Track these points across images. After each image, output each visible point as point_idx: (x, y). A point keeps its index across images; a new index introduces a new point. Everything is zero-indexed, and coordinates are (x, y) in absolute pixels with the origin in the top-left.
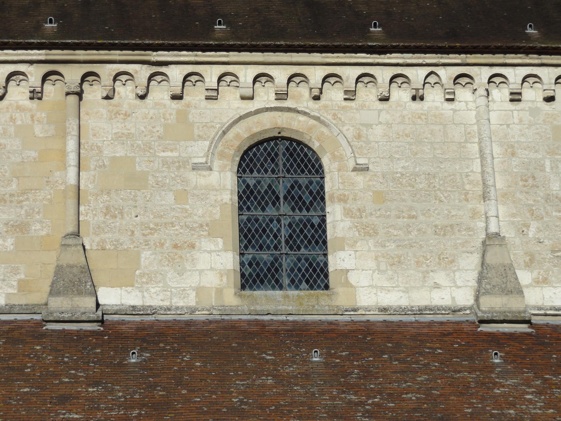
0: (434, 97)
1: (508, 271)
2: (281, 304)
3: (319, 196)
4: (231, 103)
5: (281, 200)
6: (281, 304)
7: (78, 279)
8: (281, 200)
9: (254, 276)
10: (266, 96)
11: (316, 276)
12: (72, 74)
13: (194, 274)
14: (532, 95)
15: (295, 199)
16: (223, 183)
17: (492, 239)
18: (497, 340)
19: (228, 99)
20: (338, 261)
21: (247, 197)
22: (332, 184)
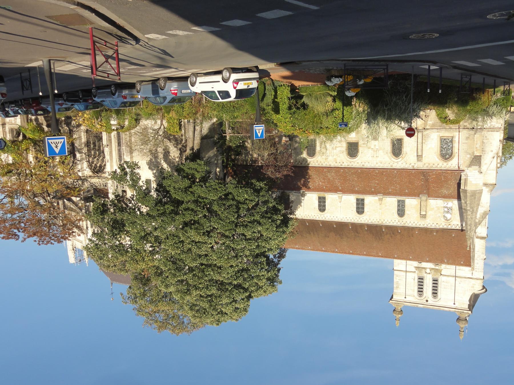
0: (345, 218)
1: (339, 199)
2: (361, 197)
3: (357, 208)
4: (365, 218)
5: (360, 208)
6: (361, 197)
7: (381, 200)
8: (360, 208)
9: (363, 200)
10: (361, 219)
11: (358, 200)
12: (380, 222)
13: (369, 200)
14: (335, 217)
15: (359, 208)
16: (366, 209)
17: (340, 202)
18: (340, 191)
19: (364, 219)
20: (355, 201)
21: (363, 208)
22: (355, 209)
